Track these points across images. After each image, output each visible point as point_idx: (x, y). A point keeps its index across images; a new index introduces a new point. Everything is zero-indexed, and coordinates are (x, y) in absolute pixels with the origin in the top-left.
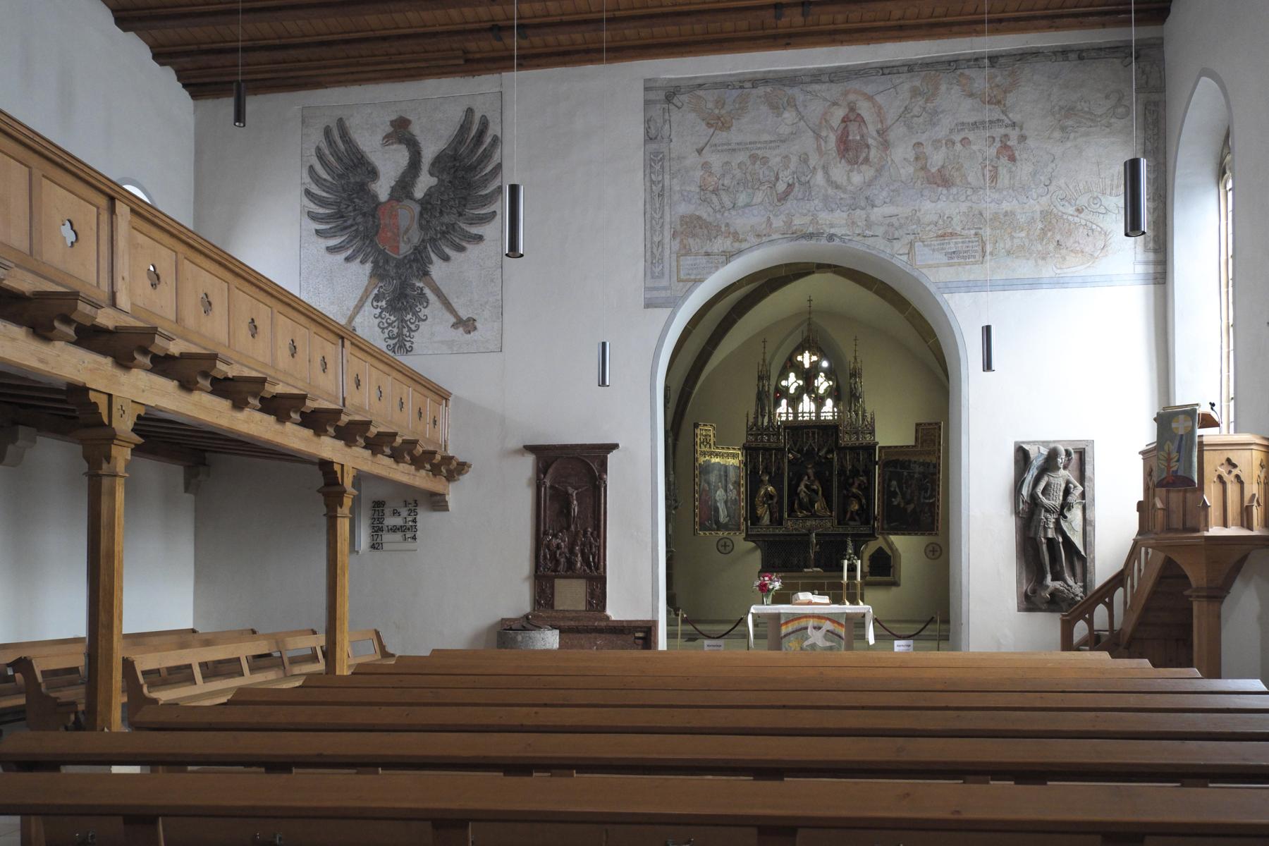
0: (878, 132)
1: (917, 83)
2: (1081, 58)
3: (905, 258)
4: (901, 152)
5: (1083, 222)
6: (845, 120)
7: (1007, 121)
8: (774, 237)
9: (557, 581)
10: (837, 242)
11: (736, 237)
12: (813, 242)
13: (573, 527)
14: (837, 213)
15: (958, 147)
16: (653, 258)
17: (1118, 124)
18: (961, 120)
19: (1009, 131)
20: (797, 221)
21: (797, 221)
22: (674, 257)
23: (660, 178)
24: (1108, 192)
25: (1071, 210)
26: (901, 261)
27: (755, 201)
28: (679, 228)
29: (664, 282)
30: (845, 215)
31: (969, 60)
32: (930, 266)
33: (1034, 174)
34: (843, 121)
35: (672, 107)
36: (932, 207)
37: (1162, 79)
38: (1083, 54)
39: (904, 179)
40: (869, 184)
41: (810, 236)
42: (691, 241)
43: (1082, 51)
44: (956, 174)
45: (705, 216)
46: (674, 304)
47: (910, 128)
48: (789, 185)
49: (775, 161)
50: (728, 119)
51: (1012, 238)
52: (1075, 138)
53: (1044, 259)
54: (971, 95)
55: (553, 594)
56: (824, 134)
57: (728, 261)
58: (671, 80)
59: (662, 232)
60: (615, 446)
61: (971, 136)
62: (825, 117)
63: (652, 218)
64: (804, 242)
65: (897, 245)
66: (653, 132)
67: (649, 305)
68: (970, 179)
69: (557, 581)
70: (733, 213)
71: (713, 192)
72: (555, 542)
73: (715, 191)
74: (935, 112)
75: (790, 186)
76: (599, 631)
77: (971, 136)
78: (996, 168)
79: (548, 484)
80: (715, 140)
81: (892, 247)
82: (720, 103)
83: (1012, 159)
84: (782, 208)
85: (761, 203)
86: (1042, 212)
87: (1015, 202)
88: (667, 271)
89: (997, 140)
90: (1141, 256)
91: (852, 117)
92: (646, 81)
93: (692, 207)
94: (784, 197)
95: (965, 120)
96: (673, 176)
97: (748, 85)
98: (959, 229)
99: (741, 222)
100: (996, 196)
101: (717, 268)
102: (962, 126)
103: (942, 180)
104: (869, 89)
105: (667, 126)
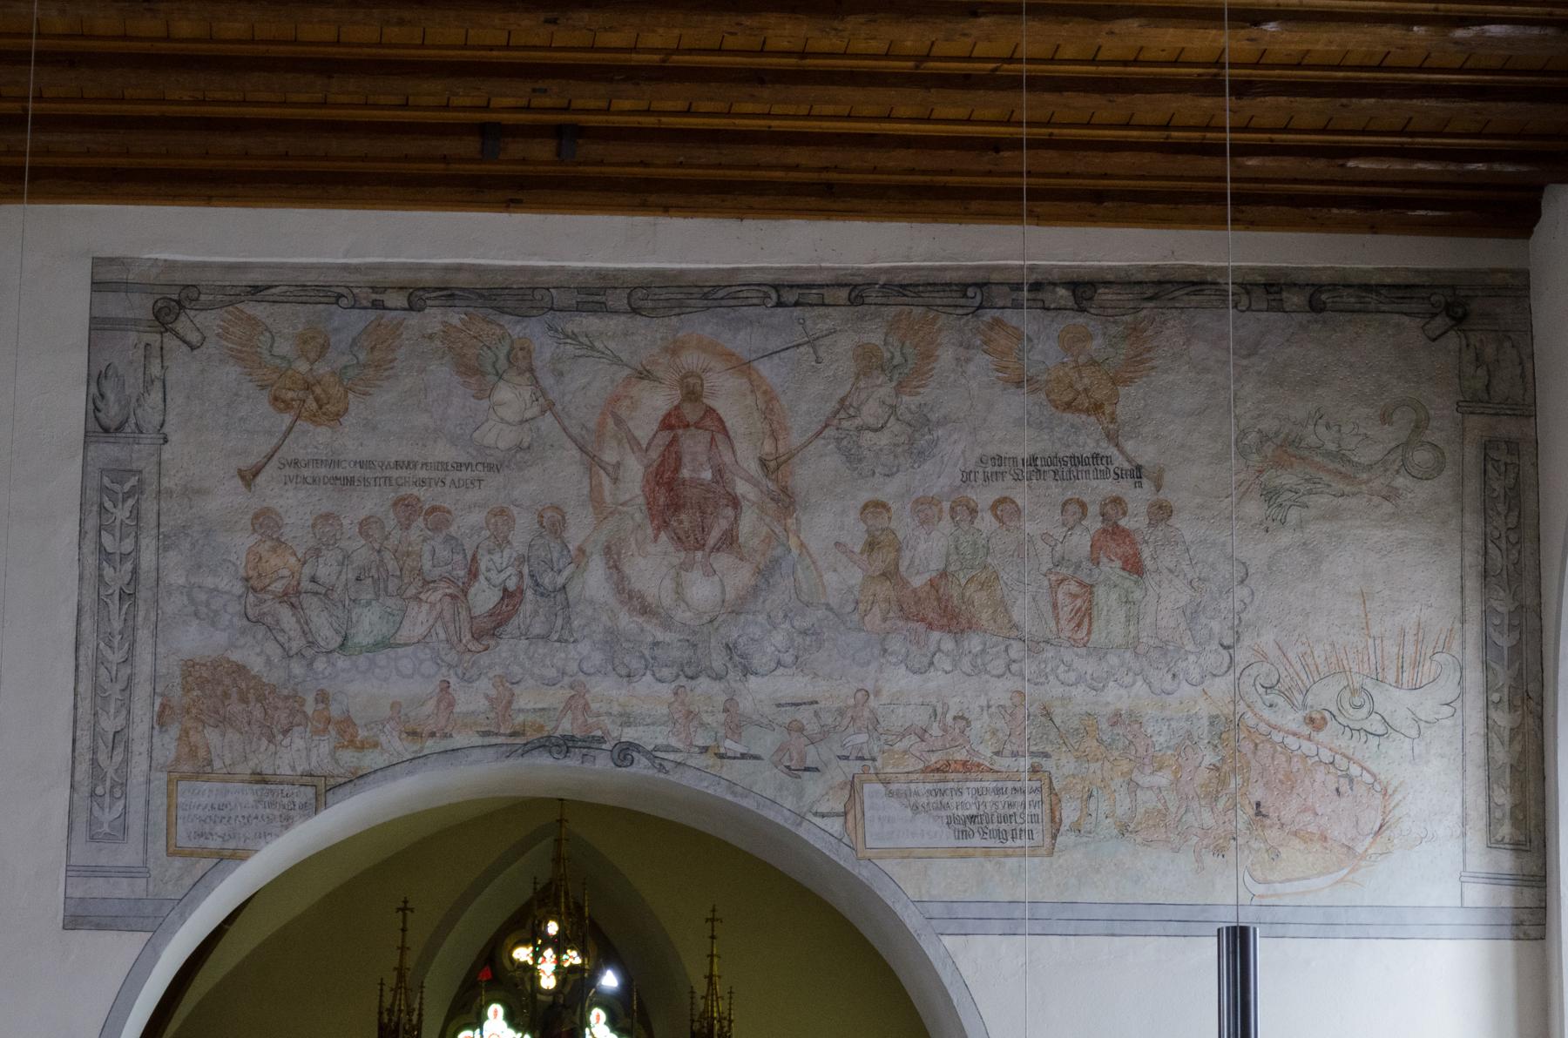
0: (763, 463)
2: (1315, 307)
3: (835, 825)
4: (829, 525)
5: (1326, 756)
6: (671, 422)
7: (1119, 461)
8: (459, 740)
10: (641, 767)
11: (346, 732)
12: (573, 762)
14: (645, 684)
15: (986, 522)
16: (97, 781)
17: (1419, 493)
18: (992, 450)
19: (1125, 488)
20: (527, 700)
21: (527, 700)
22: (160, 779)
23: (128, 546)
24: (1391, 678)
25: (1292, 720)
26: (821, 833)
27: (405, 634)
29: (129, 854)
30: (665, 690)
31: (1017, 287)
32: (906, 854)
33: (1192, 614)
35: (171, 342)
36: (918, 686)
37: (1527, 378)
38: (1320, 297)
39: (834, 602)
40: (737, 610)
41: (565, 745)
42: (212, 736)
43: (1319, 288)
44: (980, 597)
45: (256, 665)
46: (153, 920)
47: (853, 458)
50: (336, 391)
51: (1133, 786)
52: (1301, 525)
53: (1219, 851)
56: (610, 456)
57: (319, 804)
58: (171, 266)
59: (126, 706)
61: (1022, 495)
63: (99, 661)
64: (544, 760)
65: (813, 787)
66: (112, 413)
67: (75, 920)
68: (1016, 615)
70: (342, 662)
71: (284, 597)
73: (291, 597)
74: (922, 422)
75: (510, 596)
77: (1022, 495)
78: (1089, 588)
80: (291, 450)
81: (800, 794)
82: (315, 343)
83: (1134, 566)
84: (485, 660)
85: (423, 641)
86: (1213, 720)
89: (1093, 509)
90: (1479, 859)
91: (691, 416)
92: (97, 262)
93: (221, 638)
94: (491, 628)
95: (1007, 450)
96: (165, 544)
97: (396, 299)
98: (986, 751)
99: (366, 689)
100: (1089, 666)
101: (287, 823)
103: (941, 612)
104: (743, 342)
105: (155, 396)
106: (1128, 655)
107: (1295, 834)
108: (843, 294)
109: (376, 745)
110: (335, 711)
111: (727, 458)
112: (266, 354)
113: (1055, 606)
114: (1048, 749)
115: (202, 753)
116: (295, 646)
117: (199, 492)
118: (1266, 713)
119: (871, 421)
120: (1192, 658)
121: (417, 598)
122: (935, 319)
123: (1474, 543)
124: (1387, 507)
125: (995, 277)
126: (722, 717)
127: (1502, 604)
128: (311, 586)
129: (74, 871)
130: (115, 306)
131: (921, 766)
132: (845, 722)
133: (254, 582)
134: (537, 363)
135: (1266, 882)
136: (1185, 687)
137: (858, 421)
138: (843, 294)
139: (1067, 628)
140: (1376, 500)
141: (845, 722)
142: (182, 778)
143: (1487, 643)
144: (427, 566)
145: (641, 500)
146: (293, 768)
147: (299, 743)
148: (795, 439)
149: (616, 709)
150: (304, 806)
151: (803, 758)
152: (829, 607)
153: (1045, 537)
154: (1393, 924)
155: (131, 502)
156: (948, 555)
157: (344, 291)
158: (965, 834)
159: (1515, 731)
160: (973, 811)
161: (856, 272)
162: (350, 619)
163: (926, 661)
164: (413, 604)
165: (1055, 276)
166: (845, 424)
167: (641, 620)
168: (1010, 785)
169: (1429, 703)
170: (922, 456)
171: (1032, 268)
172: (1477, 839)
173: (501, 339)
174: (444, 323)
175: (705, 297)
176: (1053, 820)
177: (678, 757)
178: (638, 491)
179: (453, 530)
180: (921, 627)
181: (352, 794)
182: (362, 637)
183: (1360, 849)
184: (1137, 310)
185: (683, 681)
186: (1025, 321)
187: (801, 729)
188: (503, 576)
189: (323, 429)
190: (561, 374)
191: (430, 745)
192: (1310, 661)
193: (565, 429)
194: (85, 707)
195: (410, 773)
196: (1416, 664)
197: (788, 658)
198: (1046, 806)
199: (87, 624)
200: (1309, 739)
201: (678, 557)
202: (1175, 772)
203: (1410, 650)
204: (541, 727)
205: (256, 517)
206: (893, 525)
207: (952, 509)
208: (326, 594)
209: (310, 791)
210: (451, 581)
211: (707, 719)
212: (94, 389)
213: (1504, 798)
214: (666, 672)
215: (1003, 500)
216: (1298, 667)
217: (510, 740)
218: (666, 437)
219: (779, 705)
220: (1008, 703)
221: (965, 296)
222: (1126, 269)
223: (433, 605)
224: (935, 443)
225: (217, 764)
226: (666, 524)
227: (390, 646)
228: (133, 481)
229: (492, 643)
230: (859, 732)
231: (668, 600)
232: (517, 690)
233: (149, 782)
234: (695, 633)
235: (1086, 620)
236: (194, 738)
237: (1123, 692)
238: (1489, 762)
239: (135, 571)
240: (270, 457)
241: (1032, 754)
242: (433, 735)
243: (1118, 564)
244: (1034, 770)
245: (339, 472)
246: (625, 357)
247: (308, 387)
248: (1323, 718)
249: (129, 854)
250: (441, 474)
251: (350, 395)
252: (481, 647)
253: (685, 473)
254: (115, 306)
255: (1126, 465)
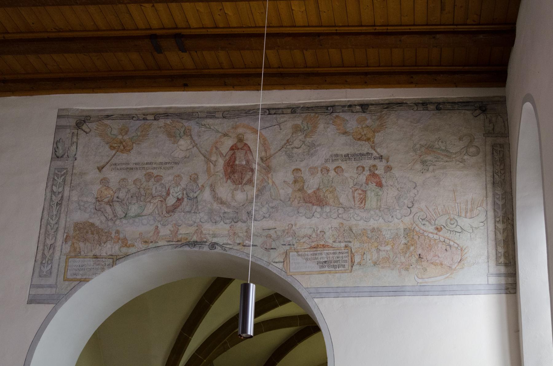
0: (262, 159)
1: (298, 121)
2: (438, 109)
3: (280, 266)
4: (282, 177)
5: (442, 239)
7: (375, 154)
8: (160, 243)
10: (218, 250)
11: (125, 243)
12: (196, 249)
15: (332, 173)
18: (335, 152)
19: (377, 162)
21: (183, 231)
22: (64, 258)
23: (61, 190)
24: (463, 215)
25: (431, 229)
27: (145, 212)
28: (71, 233)
29: (51, 281)
30: (227, 227)
32: (303, 274)
33: (398, 198)
34: (232, 149)
35: (80, 132)
36: (308, 223)
38: (439, 106)
39: (282, 199)
41: (195, 244)
42: (82, 245)
44: (330, 196)
45: (97, 223)
47: (290, 156)
48: (178, 199)
49: (168, 178)
50: (130, 143)
52: (434, 170)
53: (407, 269)
54: (345, 133)
56: (213, 158)
57: (114, 264)
58: (83, 111)
61: (344, 165)
62: (216, 146)
63: (48, 223)
64: (187, 248)
65: (274, 255)
66: (60, 152)
67: (30, 302)
70: (124, 221)
73: (110, 203)
74: (313, 145)
75: (179, 200)
78: (365, 192)
80: (114, 161)
82: (124, 131)
83: (380, 185)
86: (405, 230)
87: (381, 220)
88: (55, 271)
89: (367, 169)
91: (240, 146)
92: (60, 110)
93: (87, 216)
95: (339, 152)
96: (72, 189)
97: (152, 117)
99: (130, 230)
100: (364, 215)
101: (103, 270)
102: (335, 157)
103: (317, 200)
105: (74, 147)
106: (377, 211)
107: (432, 263)
108: (289, 111)
109: (133, 246)
110: (121, 236)
111: (251, 158)
112: (109, 135)
113: (354, 197)
114: (351, 240)
115: (78, 250)
116: (110, 217)
117: (85, 173)
118: (422, 227)
119: (297, 146)
120: (398, 211)
121: (150, 202)
122: (318, 116)
123: (490, 174)
124: (462, 165)
125: (337, 104)
126: (245, 234)
127: (499, 192)
128: (117, 200)
129: (32, 286)
130: (63, 122)
131: (309, 246)
132: (285, 234)
133: (99, 199)
134: (193, 133)
135: (422, 278)
136: (396, 220)
137: (292, 146)
138: (289, 111)
139: (358, 204)
140: (458, 163)
141: (285, 234)
142: (71, 258)
143: (494, 203)
144: (154, 192)
145: (223, 171)
146: (107, 254)
147: (109, 246)
148: (272, 152)
149: (211, 232)
150: (109, 265)
151: (271, 245)
152: (281, 200)
153: (351, 177)
154: (466, 290)
155: (63, 177)
156: (320, 183)
157: (135, 116)
158: (323, 267)
159: (504, 230)
160: (326, 260)
161: (294, 104)
162: (128, 209)
163: (311, 215)
164: (149, 204)
165: (356, 103)
166: (288, 147)
167: (220, 206)
168: (338, 251)
169: (475, 222)
170: (312, 155)
171: (349, 101)
172: (492, 263)
173: (182, 127)
174: (164, 123)
175: (246, 113)
176: (352, 261)
177: (231, 247)
178: (222, 168)
179: (163, 182)
180: (310, 205)
181: (124, 261)
182: (132, 213)
183: (454, 267)
184: (381, 112)
185: (233, 223)
186: (346, 116)
187: (270, 237)
188: (178, 194)
189: (124, 154)
190: (200, 136)
191: (151, 245)
192: (437, 211)
193: (200, 152)
194: (42, 237)
195: (143, 254)
196: (472, 210)
197: (267, 215)
198: (350, 258)
199: (46, 212)
200: (436, 234)
201: (233, 187)
202: (392, 246)
203: (469, 207)
204: (187, 239)
205: (102, 180)
206: (302, 175)
207: (321, 170)
208: (121, 202)
209: (111, 261)
210: (161, 196)
211: (240, 235)
212: (55, 146)
213: (501, 250)
214: (228, 221)
215: (338, 167)
216: (433, 213)
217: (177, 243)
218: (232, 152)
219: (263, 230)
220: (338, 227)
221: (327, 109)
222: (378, 100)
223: (155, 203)
224: (316, 151)
225: (82, 253)
226: (230, 178)
227: (140, 216)
228: (65, 171)
229: (172, 214)
230: (289, 236)
231: (229, 199)
232: (180, 228)
233: (60, 259)
234: (237, 209)
235: (364, 201)
236: (76, 245)
237: (375, 222)
238: (496, 239)
239: (62, 197)
240: (107, 163)
241: (346, 242)
242: (152, 242)
243: (375, 184)
244: (346, 247)
245: (129, 166)
246: (220, 130)
247: (121, 143)
248: (441, 228)
249: (51, 281)
250: (160, 166)
251: (134, 145)
252: (169, 215)
253: (237, 162)
254: (63, 122)
255: (377, 156)
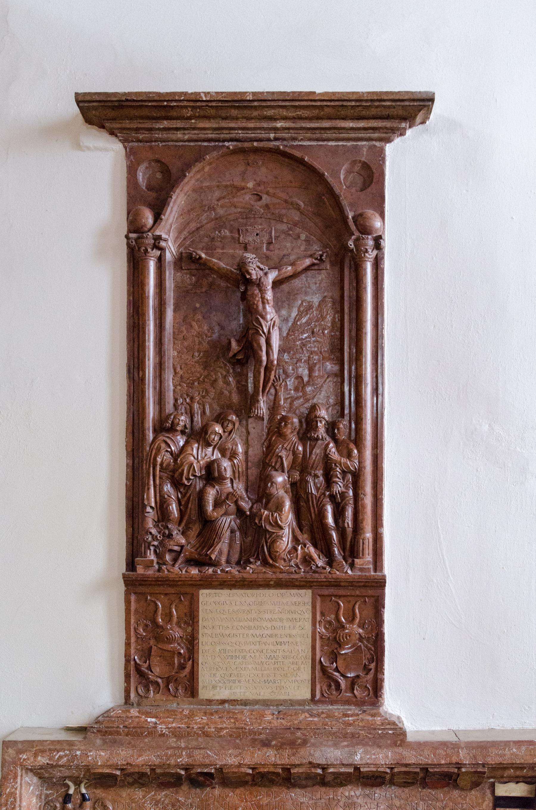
9: (206, 597)
13: (263, 406)
55: (192, 642)
60: (407, 110)
69: (206, 597)
72: (199, 456)
76: (372, 779)
79: (171, 250)
